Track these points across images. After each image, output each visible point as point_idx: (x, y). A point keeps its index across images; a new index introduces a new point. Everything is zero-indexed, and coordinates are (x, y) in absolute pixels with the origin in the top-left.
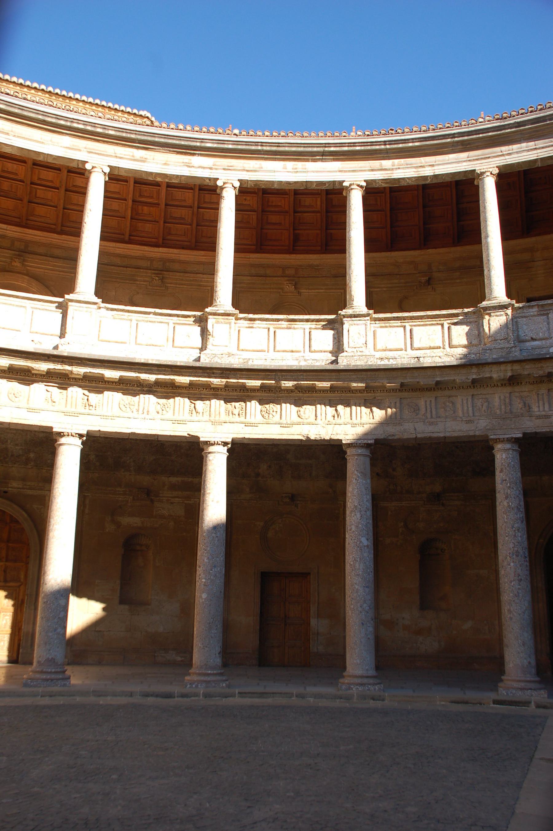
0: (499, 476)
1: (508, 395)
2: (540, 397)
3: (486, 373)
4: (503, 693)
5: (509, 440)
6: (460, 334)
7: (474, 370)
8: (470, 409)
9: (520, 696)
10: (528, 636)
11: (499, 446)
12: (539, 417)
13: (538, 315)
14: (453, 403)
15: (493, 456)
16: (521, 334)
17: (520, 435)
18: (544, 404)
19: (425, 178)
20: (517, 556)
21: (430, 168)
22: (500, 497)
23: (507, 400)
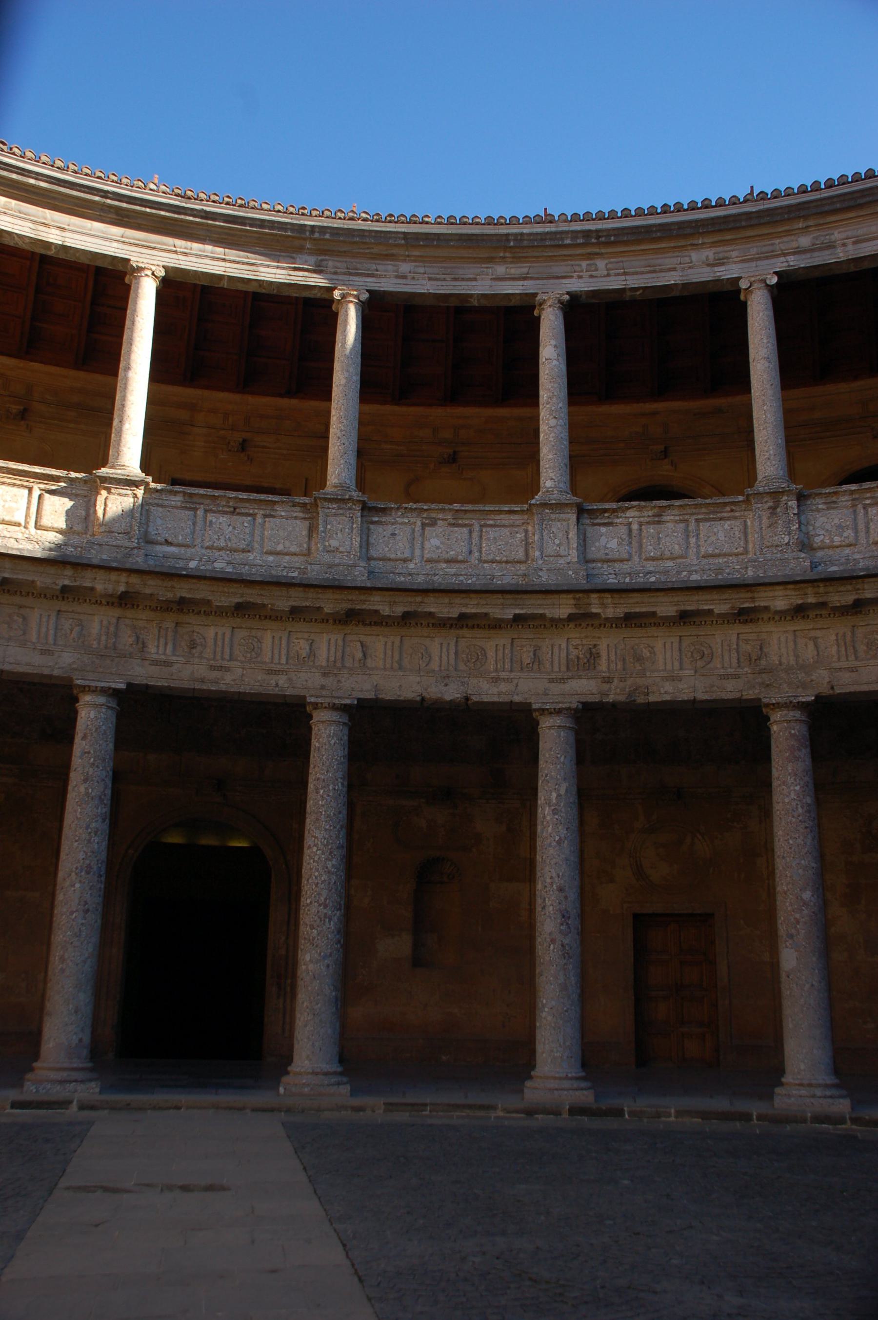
0: (80, 745)
1: (114, 621)
2: (163, 632)
3: (87, 580)
4: (30, 1090)
5: (104, 691)
6: (56, 510)
7: (69, 572)
8: (52, 632)
9: (57, 1092)
10: (84, 998)
11: (87, 698)
12: (155, 663)
13: (182, 508)
14: (24, 619)
15: (76, 712)
16: (152, 530)
17: (123, 686)
18: (166, 644)
19: (48, 245)
20: (88, 873)
21: (57, 232)
22: (75, 777)
23: (112, 629)
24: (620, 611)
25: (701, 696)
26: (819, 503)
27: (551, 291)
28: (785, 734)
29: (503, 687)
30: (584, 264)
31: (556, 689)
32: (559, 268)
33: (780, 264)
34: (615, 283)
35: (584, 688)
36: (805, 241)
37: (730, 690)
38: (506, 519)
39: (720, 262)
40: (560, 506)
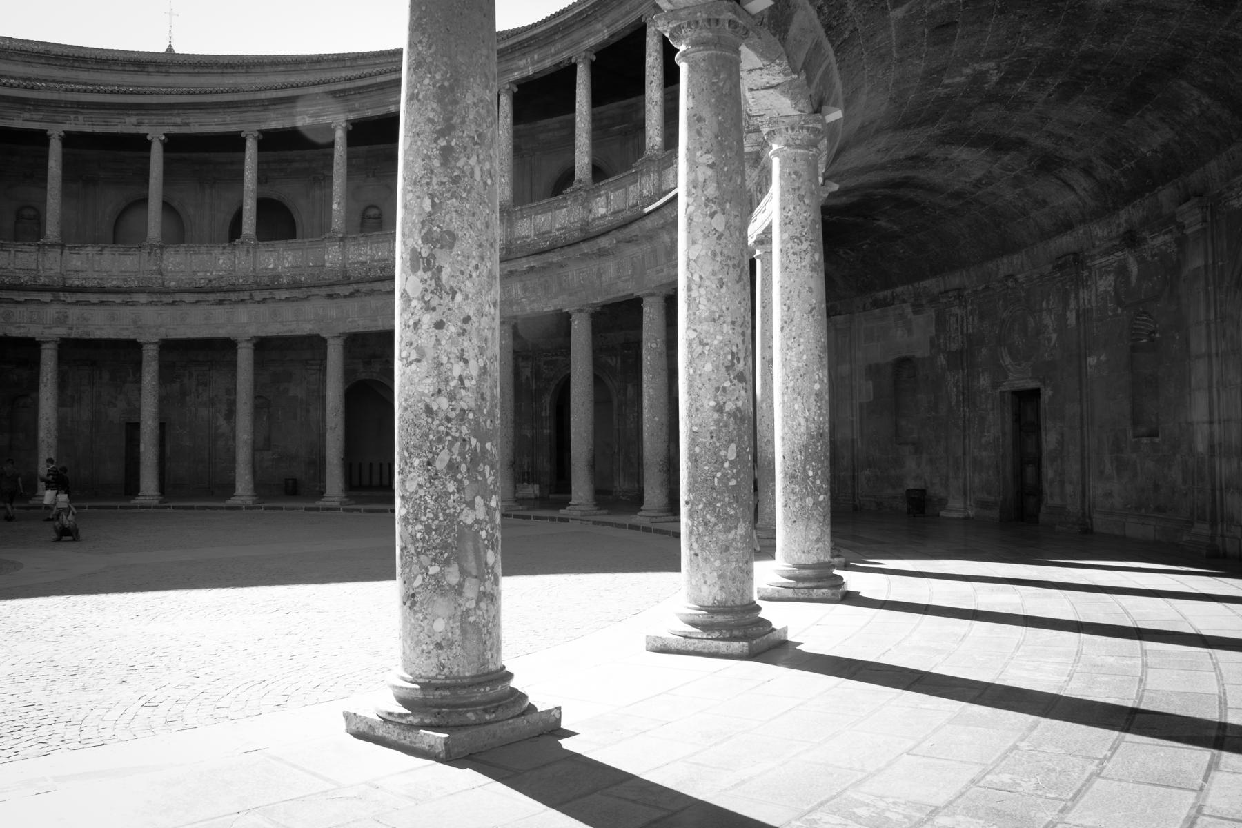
24: (74, 300)
25: (112, 337)
26: (171, 250)
27: (56, 131)
28: (150, 354)
29: (23, 330)
30: (72, 116)
31: (47, 332)
32: (59, 118)
33: (167, 130)
34: (87, 129)
35: (61, 332)
36: (178, 120)
37: (125, 335)
38: (27, 248)
39: (139, 124)
40: (52, 245)
